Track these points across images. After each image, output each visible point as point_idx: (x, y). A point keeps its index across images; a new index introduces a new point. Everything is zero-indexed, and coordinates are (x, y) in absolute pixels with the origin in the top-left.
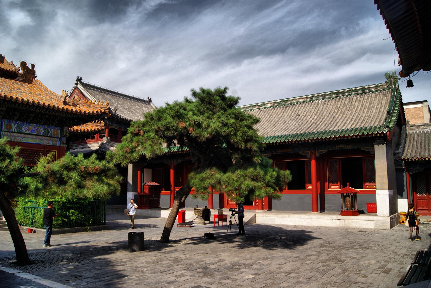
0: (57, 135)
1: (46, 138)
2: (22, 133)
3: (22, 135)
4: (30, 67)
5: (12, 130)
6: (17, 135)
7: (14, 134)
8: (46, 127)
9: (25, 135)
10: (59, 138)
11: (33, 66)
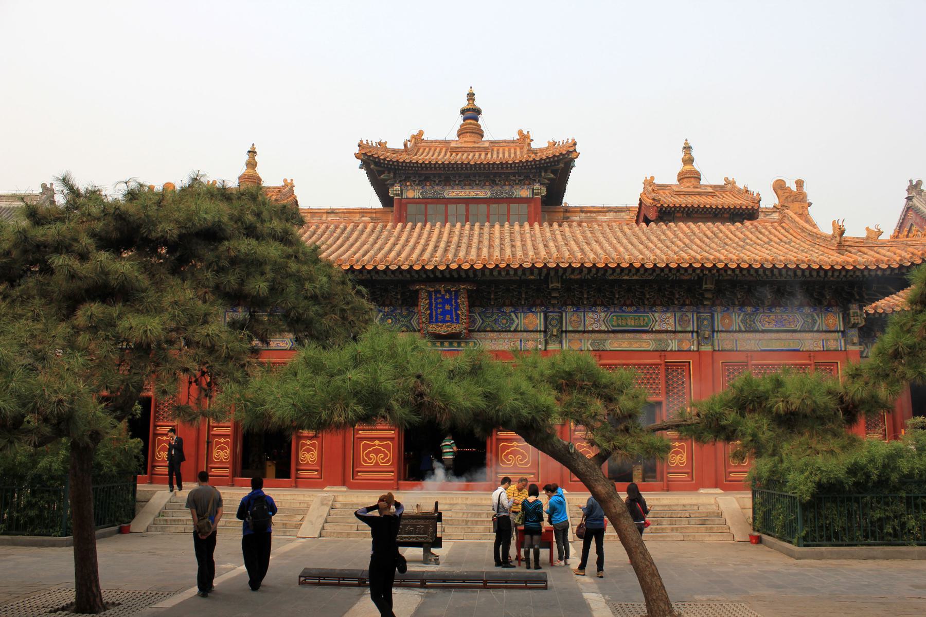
0: (835, 324)
1: (810, 335)
3: (758, 335)
4: (794, 188)
5: (735, 327)
6: (746, 335)
7: (740, 335)
10: (843, 332)
11: (800, 183)
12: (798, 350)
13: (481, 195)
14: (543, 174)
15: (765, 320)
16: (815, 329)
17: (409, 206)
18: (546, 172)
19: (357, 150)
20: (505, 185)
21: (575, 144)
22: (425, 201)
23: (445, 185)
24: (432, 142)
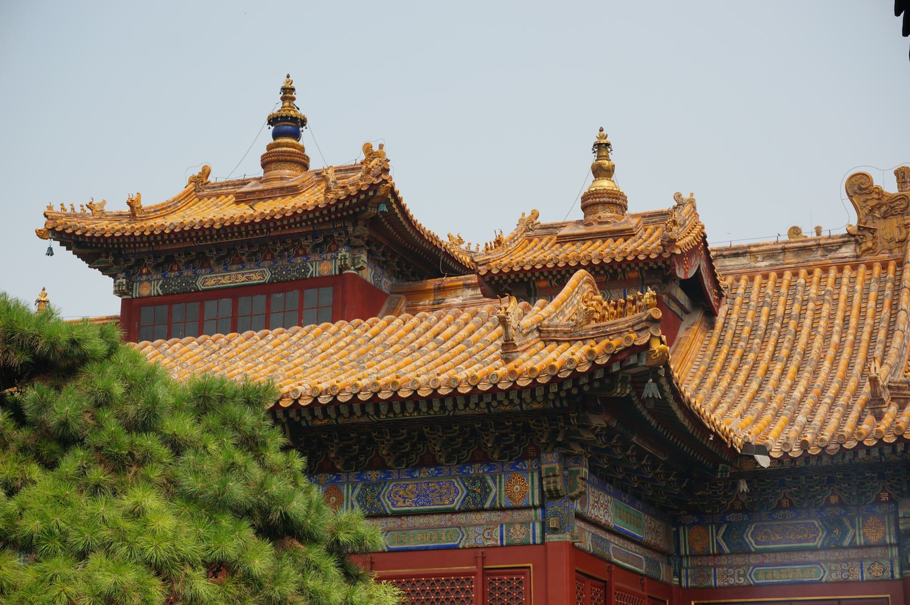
0: (524, 495)
2: (386, 516)
4: (890, 187)
8: (475, 470)
9: (398, 521)
12: (455, 548)
13: (256, 279)
14: (350, 229)
15: (399, 493)
16: (487, 505)
17: (144, 310)
18: (355, 225)
19: (41, 223)
20: (297, 255)
21: (386, 171)
22: (168, 299)
23: (201, 268)
24: (222, 185)
